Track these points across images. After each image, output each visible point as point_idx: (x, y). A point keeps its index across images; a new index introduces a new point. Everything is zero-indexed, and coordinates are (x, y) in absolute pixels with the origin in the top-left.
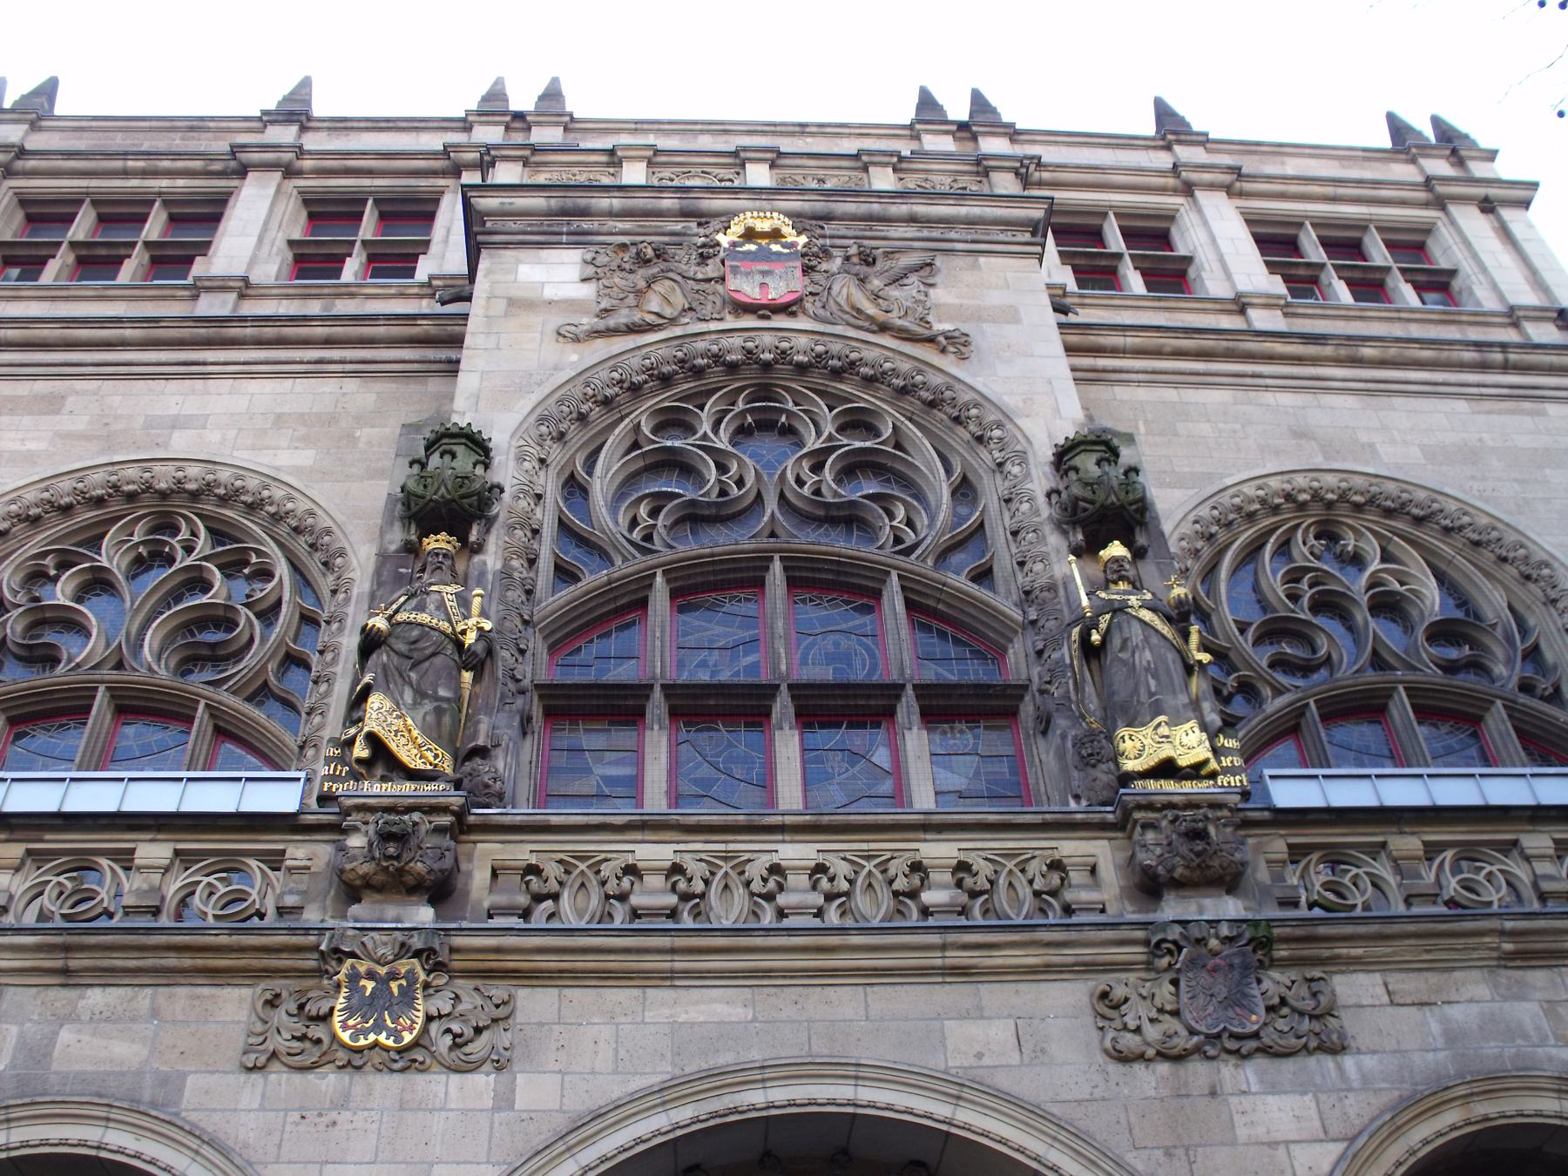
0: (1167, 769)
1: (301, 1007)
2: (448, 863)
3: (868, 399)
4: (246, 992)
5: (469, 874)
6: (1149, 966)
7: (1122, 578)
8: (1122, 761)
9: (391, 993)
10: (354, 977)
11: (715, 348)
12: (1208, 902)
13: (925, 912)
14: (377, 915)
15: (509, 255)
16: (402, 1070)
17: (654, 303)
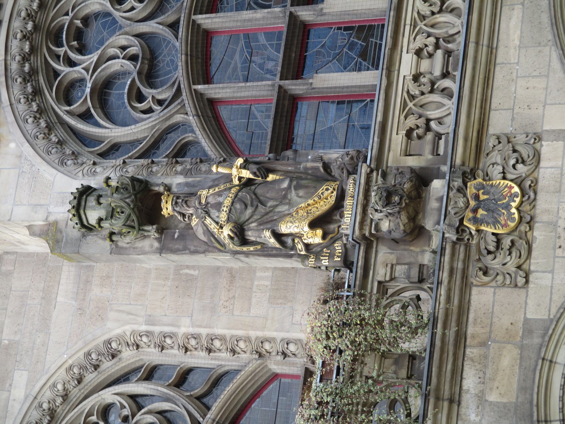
1: (489, 252)
9: (487, 199)
10: (475, 220)
11: (18, 58)
14: (436, 213)
16: (535, 193)
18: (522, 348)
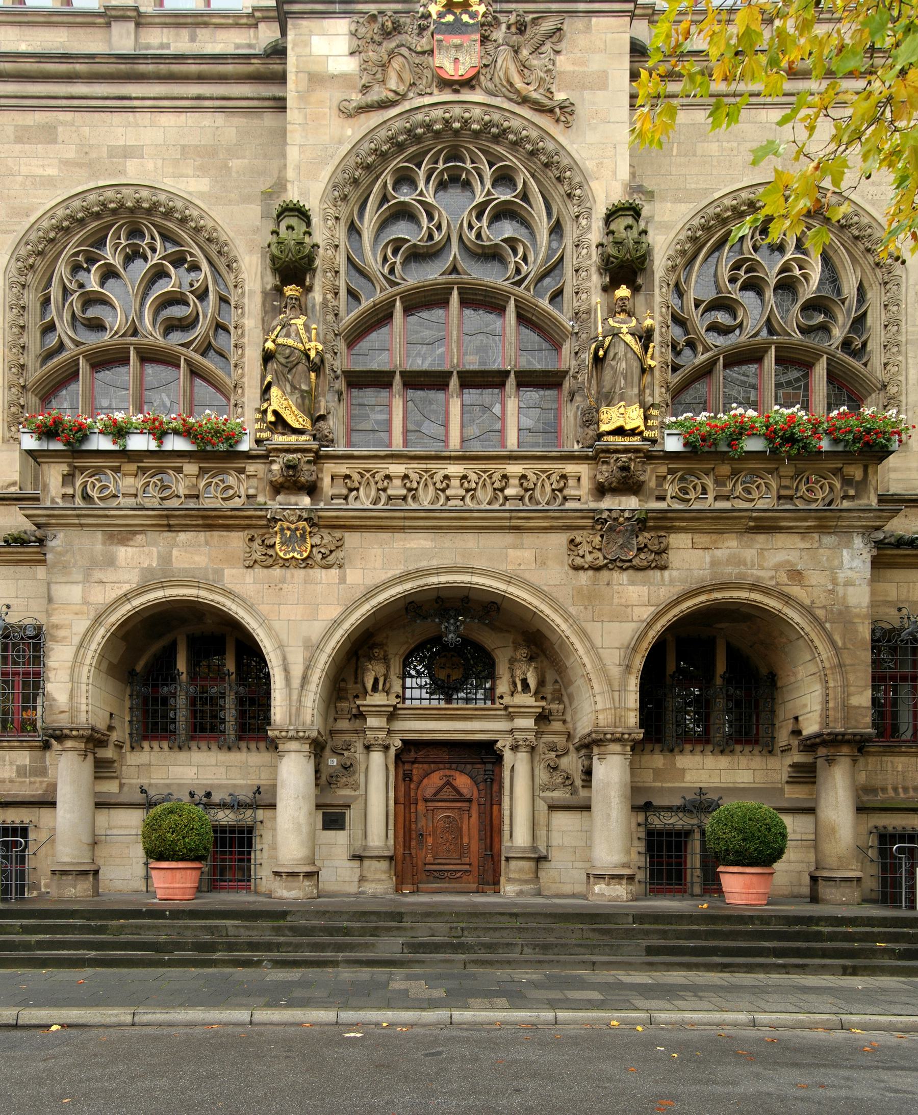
2: (314, 478)
3: (512, 160)
4: (241, 534)
5: (322, 479)
6: (593, 528)
12: (624, 499)
13: (506, 498)
15: (304, 23)
17: (393, 83)
18: (206, 569)
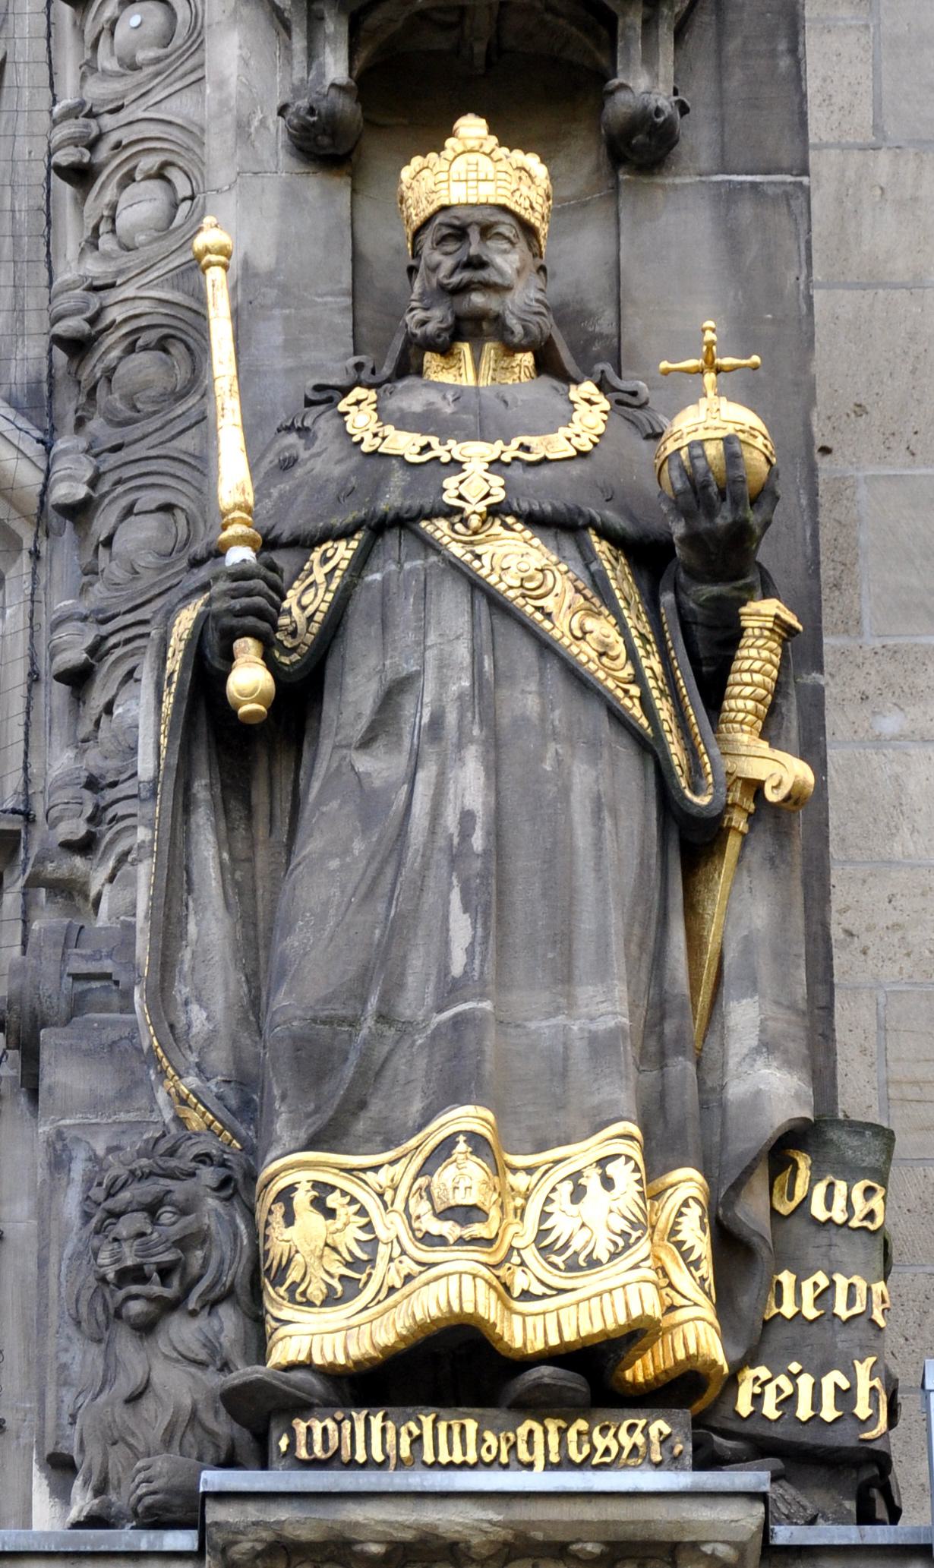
0: (451, 1368)
7: (468, 328)
8: (277, 1306)
